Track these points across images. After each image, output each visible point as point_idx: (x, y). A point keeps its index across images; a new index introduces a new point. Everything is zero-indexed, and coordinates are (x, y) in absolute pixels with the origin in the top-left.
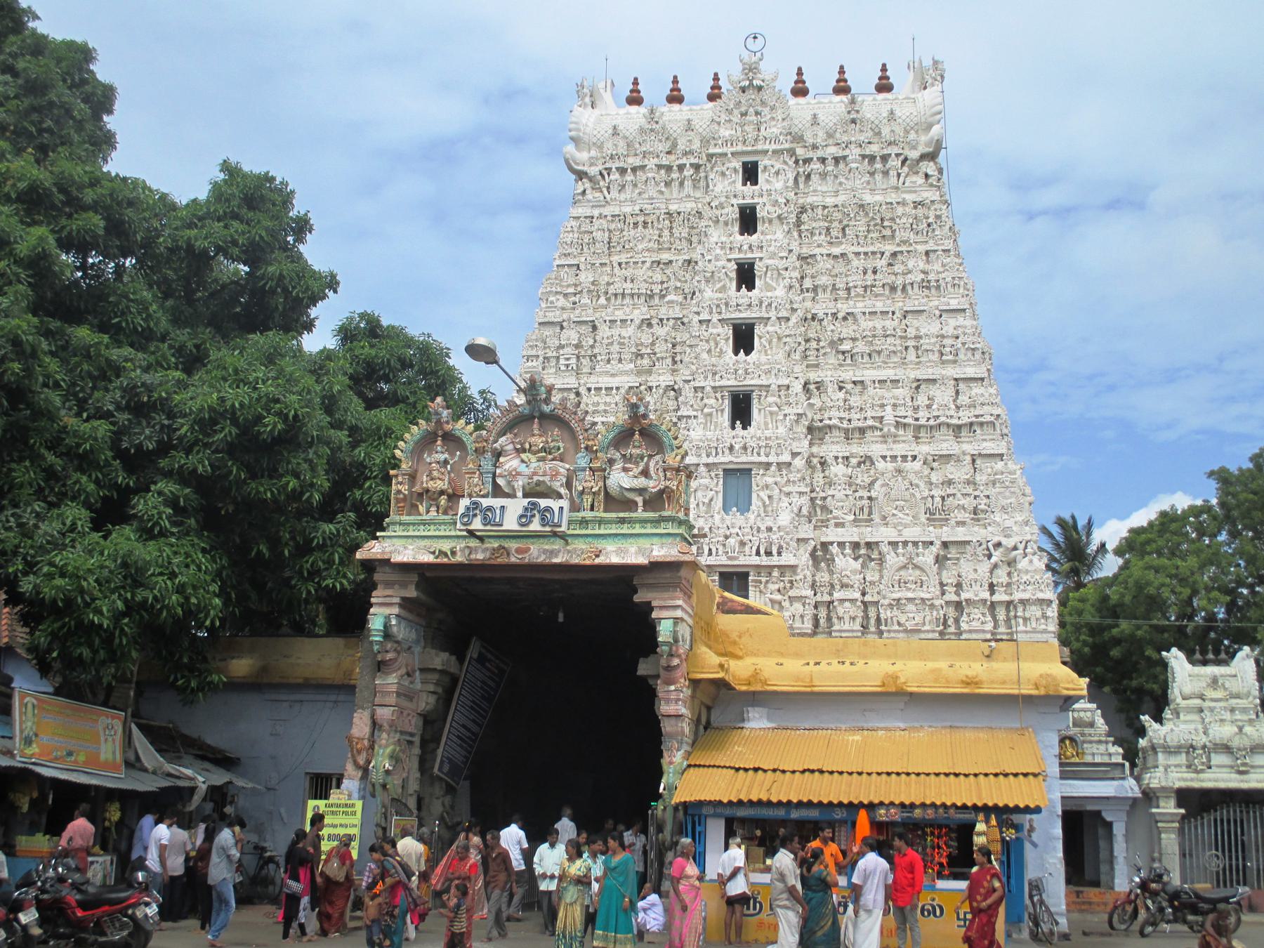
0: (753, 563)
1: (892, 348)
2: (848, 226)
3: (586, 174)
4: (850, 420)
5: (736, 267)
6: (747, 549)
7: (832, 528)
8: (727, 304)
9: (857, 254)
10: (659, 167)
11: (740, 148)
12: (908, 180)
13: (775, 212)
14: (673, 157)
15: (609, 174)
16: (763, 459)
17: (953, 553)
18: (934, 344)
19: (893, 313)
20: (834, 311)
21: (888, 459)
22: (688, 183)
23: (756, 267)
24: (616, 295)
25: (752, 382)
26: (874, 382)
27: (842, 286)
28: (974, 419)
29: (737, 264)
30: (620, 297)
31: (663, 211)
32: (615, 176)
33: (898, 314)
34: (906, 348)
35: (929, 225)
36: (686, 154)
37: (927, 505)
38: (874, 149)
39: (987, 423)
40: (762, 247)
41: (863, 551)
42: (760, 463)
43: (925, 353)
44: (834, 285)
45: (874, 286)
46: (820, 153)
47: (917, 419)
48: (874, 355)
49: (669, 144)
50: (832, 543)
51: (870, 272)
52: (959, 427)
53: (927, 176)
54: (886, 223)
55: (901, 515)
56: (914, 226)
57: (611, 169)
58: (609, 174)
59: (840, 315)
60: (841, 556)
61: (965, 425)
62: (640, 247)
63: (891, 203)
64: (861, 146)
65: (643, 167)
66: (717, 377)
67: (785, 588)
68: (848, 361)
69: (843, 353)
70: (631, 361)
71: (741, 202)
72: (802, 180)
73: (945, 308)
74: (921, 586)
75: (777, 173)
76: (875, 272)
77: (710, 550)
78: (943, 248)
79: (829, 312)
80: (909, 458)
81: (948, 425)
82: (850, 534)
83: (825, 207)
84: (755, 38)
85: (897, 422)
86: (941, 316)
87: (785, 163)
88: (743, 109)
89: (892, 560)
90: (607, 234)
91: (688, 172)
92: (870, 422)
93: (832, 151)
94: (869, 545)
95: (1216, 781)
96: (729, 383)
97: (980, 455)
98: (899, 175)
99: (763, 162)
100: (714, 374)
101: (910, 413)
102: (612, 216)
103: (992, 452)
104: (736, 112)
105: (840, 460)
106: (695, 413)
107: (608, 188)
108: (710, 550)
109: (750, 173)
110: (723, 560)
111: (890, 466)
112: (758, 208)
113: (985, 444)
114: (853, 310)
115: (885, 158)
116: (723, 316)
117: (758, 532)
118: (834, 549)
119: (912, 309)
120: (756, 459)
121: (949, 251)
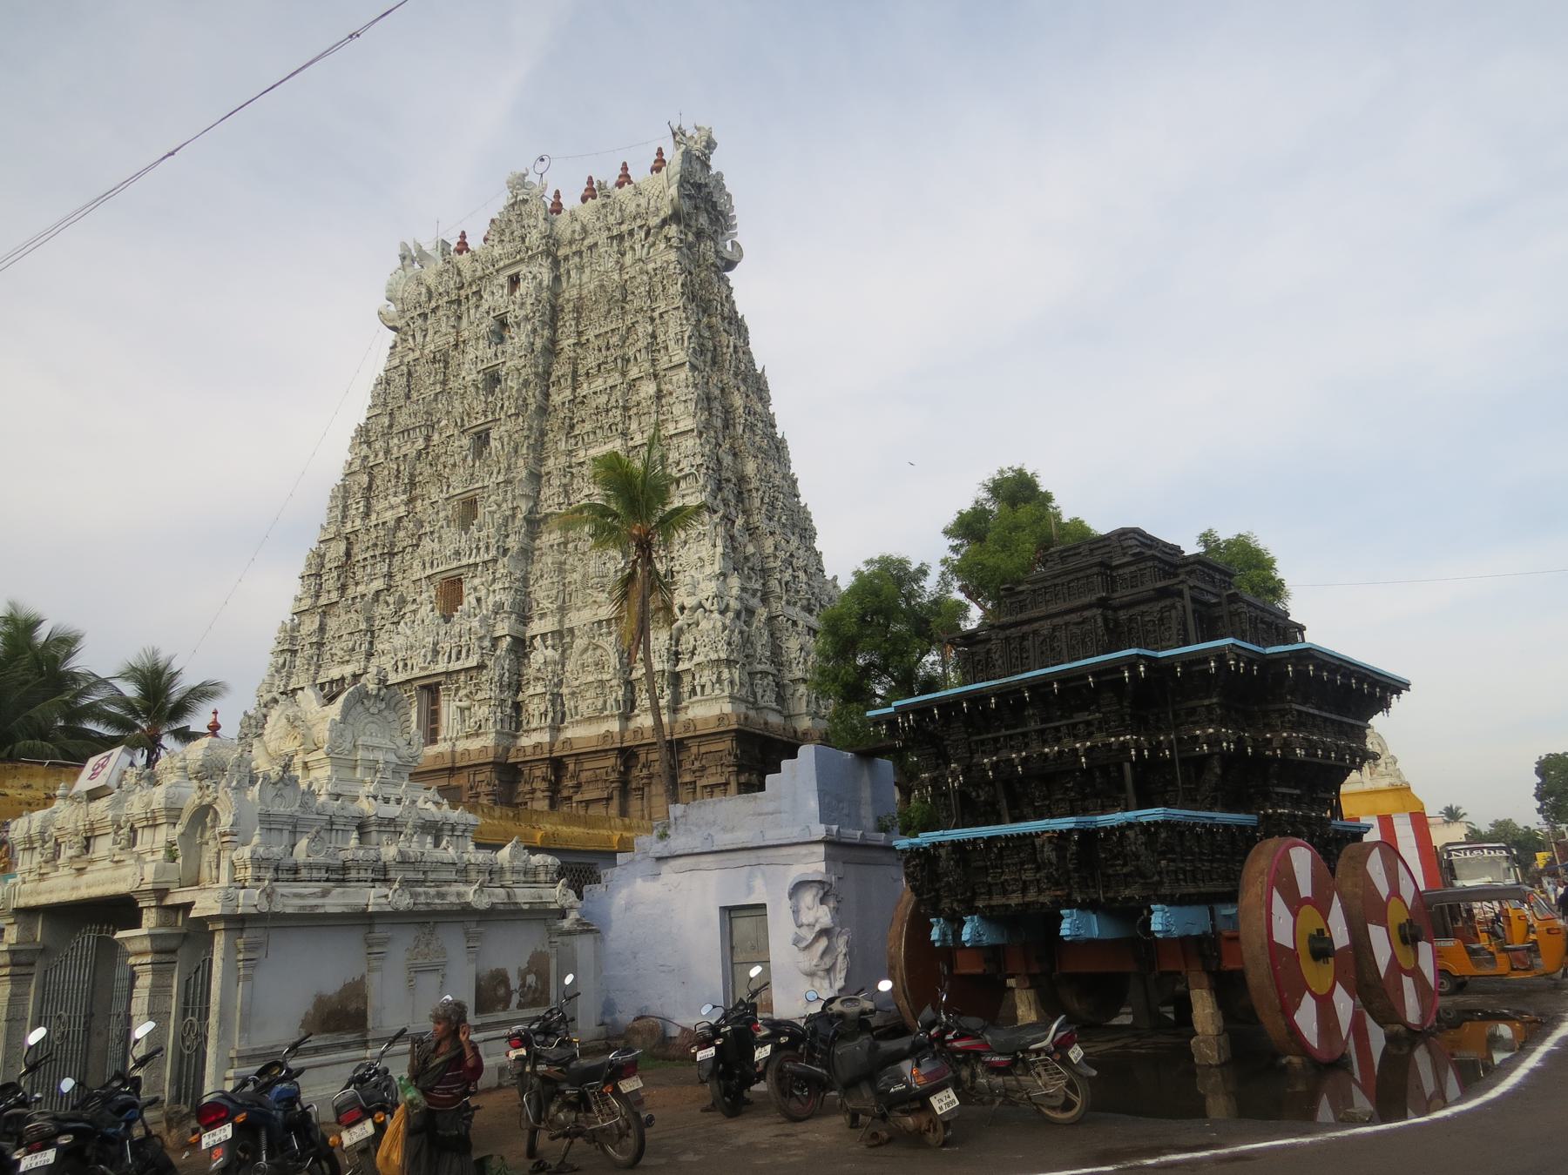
1: (611, 421)
9: (596, 336)
11: (501, 264)
12: (652, 250)
14: (462, 292)
16: (471, 561)
18: (649, 407)
24: (403, 432)
25: (476, 486)
28: (678, 475)
30: (406, 434)
32: (420, 321)
34: (630, 417)
42: (469, 566)
44: (575, 373)
45: (606, 363)
46: (574, 248)
50: (535, 636)
53: (668, 239)
59: (578, 400)
64: (609, 229)
66: (451, 489)
67: (471, 693)
68: (580, 442)
69: (575, 437)
70: (404, 492)
71: (497, 313)
72: (564, 279)
73: (666, 366)
74: (603, 668)
76: (608, 349)
79: (567, 400)
84: (542, 160)
91: (473, 300)
94: (571, 630)
95: (51, 892)
96: (458, 491)
98: (643, 246)
99: (523, 269)
100: (449, 486)
102: (414, 360)
105: (555, 547)
107: (413, 336)
109: (514, 281)
110: (417, 673)
115: (631, 233)
118: (538, 642)
119: (637, 376)
120: (464, 562)
121: (678, 308)
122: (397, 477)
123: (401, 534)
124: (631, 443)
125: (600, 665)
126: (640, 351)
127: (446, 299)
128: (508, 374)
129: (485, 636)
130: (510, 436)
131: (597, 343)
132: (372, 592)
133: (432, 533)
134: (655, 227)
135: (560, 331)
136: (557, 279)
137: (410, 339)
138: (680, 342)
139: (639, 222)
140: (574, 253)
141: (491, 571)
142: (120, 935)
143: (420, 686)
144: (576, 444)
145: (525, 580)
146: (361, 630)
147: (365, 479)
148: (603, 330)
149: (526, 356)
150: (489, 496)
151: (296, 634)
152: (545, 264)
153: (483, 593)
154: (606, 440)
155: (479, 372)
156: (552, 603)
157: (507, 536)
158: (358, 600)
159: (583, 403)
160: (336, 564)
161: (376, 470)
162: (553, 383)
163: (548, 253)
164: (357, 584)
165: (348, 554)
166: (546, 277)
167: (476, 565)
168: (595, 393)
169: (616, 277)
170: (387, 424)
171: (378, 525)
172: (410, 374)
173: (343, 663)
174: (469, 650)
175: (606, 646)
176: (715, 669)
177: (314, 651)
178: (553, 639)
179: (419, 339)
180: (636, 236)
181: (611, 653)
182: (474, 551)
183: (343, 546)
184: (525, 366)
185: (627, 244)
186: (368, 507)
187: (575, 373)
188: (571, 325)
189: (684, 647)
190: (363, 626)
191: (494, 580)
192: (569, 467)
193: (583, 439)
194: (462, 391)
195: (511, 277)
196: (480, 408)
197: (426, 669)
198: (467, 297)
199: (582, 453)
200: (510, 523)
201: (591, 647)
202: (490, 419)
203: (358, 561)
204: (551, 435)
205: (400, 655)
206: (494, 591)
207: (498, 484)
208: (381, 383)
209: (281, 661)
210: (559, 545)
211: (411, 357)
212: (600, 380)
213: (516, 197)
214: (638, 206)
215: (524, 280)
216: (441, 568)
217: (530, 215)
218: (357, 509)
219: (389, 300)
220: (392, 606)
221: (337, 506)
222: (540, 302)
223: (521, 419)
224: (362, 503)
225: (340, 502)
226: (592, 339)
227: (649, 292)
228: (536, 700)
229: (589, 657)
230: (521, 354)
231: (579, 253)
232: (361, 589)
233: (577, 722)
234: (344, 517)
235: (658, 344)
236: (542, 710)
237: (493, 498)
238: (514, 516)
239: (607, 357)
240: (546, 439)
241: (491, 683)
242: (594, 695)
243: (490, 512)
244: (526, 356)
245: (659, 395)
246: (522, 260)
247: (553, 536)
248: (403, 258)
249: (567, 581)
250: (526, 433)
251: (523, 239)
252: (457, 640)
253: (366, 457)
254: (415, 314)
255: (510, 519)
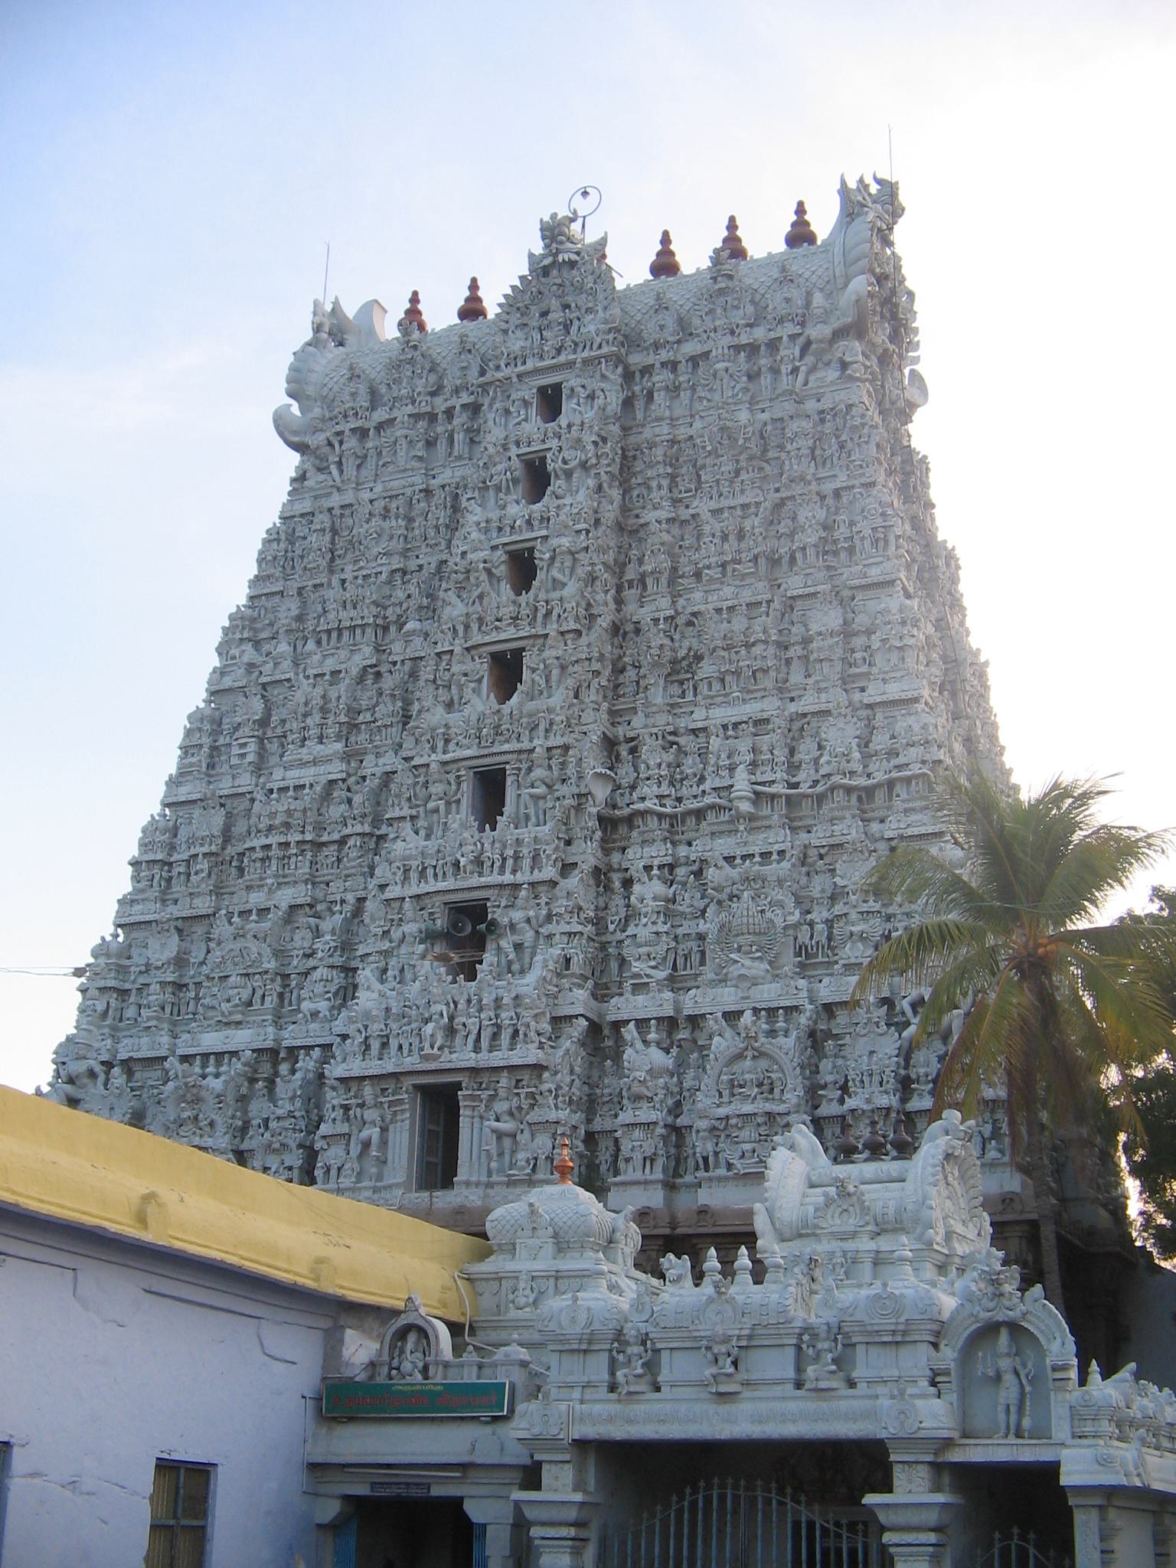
0: (463, 1065)
1: (758, 664)
2: (704, 466)
3: (307, 447)
4: (679, 800)
5: (504, 558)
6: (459, 1039)
7: (627, 995)
8: (481, 620)
10: (416, 417)
11: (530, 365)
12: (812, 378)
13: (574, 457)
15: (341, 443)
16: (508, 878)
17: (842, 1018)
19: (769, 602)
20: (672, 612)
21: (738, 861)
22: (459, 437)
23: (537, 554)
24: (329, 632)
25: (506, 747)
26: (725, 727)
27: (688, 569)
28: (894, 774)
29: (506, 552)
30: (334, 635)
31: (417, 488)
32: (351, 443)
33: (776, 605)
34: (788, 662)
35: (842, 447)
36: (457, 391)
37: (800, 940)
38: (760, 334)
39: (916, 777)
40: (548, 519)
41: (683, 1034)
42: (501, 886)
43: (818, 666)
44: (674, 569)
46: (664, 355)
47: (796, 786)
48: (728, 678)
49: (433, 378)
50: (628, 1021)
51: (731, 538)
52: (870, 791)
54: (771, 454)
55: (748, 963)
56: (818, 452)
57: (342, 432)
58: (341, 443)
59: (681, 620)
60: (639, 1045)
61: (878, 786)
62: (375, 550)
63: (781, 419)
64: (732, 333)
65: (391, 422)
66: (452, 746)
67: (520, 1108)
68: (690, 697)
70: (338, 737)
72: (639, 404)
73: (857, 582)
74: (771, 1091)
75: (592, 397)
76: (741, 536)
77: (400, 1047)
78: (863, 480)
79: (662, 615)
80: (775, 856)
81: (849, 790)
82: (658, 1003)
83: (673, 442)
84: (585, 194)
85: (755, 792)
86: (853, 599)
87: (603, 376)
88: (544, 306)
89: (722, 1044)
90: (328, 537)
92: (709, 800)
93: (690, 348)
94: (695, 1021)
96: (468, 753)
97: (902, 837)
99: (571, 381)
100: (447, 741)
101: (780, 775)
102: (342, 507)
103: (923, 830)
104: (535, 311)
105: (655, 872)
106: (414, 812)
107: (340, 464)
108: (400, 1047)
109: (551, 402)
110: (411, 1062)
111: (734, 873)
112: (549, 455)
113: (914, 817)
114: (702, 608)
115: (773, 345)
116: (477, 638)
117: (480, 1010)
118: (630, 1032)
119: (800, 592)
120: (495, 878)
122: (324, 711)
123: (336, 811)
124: (793, 708)
125: (767, 1087)
126: (804, 549)
127: (410, 409)
128: (553, 559)
129: (543, 1013)
130: (563, 668)
131: (718, 527)
132: (284, 906)
133: (412, 818)
134: (821, 341)
135: (635, 493)
136: (628, 403)
137: (334, 469)
138: (881, 544)
139: (790, 329)
140: (663, 365)
141: (543, 900)
142: (869, 1499)
143: (415, 1086)
144: (683, 695)
145: (599, 923)
146: (266, 972)
147: (257, 706)
148: (724, 503)
149: (588, 532)
150: (530, 770)
151: (127, 962)
152: (612, 377)
153: (528, 936)
154: (747, 697)
155: (494, 548)
156: (653, 967)
157: (568, 843)
158: (254, 917)
159: (690, 624)
160: (205, 849)
161: (275, 692)
162: (630, 583)
163: (618, 360)
164: (249, 888)
165: (227, 836)
166: (614, 399)
167: (516, 887)
168: (719, 611)
169: (744, 416)
170: (295, 612)
171: (286, 789)
172: (334, 532)
173: (227, 1024)
174: (516, 1032)
175: (780, 1056)
176: (987, 1115)
177: (169, 998)
178: (658, 1031)
179: (350, 470)
180: (782, 352)
181: (788, 1067)
182: (510, 862)
183: (218, 819)
184: (587, 549)
185: (764, 362)
186: (262, 755)
187: (674, 569)
188: (660, 487)
189: (922, 1071)
190: (271, 965)
191: (549, 917)
192: (671, 733)
193: (695, 689)
194: (461, 577)
195: (542, 391)
196: (507, 611)
197: (435, 1058)
198: (449, 413)
199: (699, 714)
200: (572, 820)
201: (749, 1053)
202: (522, 634)
203: (253, 849)
204: (631, 674)
205: (376, 1028)
206: (550, 936)
207: (549, 749)
208: (278, 540)
209: (101, 1007)
210: (661, 867)
211: (335, 500)
212: (728, 591)
213: (556, 255)
214: (787, 300)
215: (570, 397)
216: (442, 885)
217: (580, 289)
218: (243, 756)
219: (291, 395)
220: (328, 937)
221: (201, 746)
222: (604, 440)
223: (584, 640)
224: (252, 747)
225: (206, 740)
226: (706, 516)
227: (813, 450)
228: (637, 1133)
229: (747, 1069)
230: (578, 527)
231: (673, 366)
232: (257, 899)
233: (720, 1179)
234: (211, 766)
235: (835, 542)
236: (649, 1151)
237: (539, 773)
238: (579, 808)
239: (739, 552)
240: (621, 679)
241: (556, 1097)
242: (754, 1136)
243: (532, 796)
244: (588, 532)
245: (847, 632)
246: (571, 364)
247: (650, 851)
248: (317, 329)
249: (680, 931)
250: (596, 666)
251: (567, 327)
252: (492, 1014)
253: (251, 666)
254: (346, 427)
255: (573, 811)
